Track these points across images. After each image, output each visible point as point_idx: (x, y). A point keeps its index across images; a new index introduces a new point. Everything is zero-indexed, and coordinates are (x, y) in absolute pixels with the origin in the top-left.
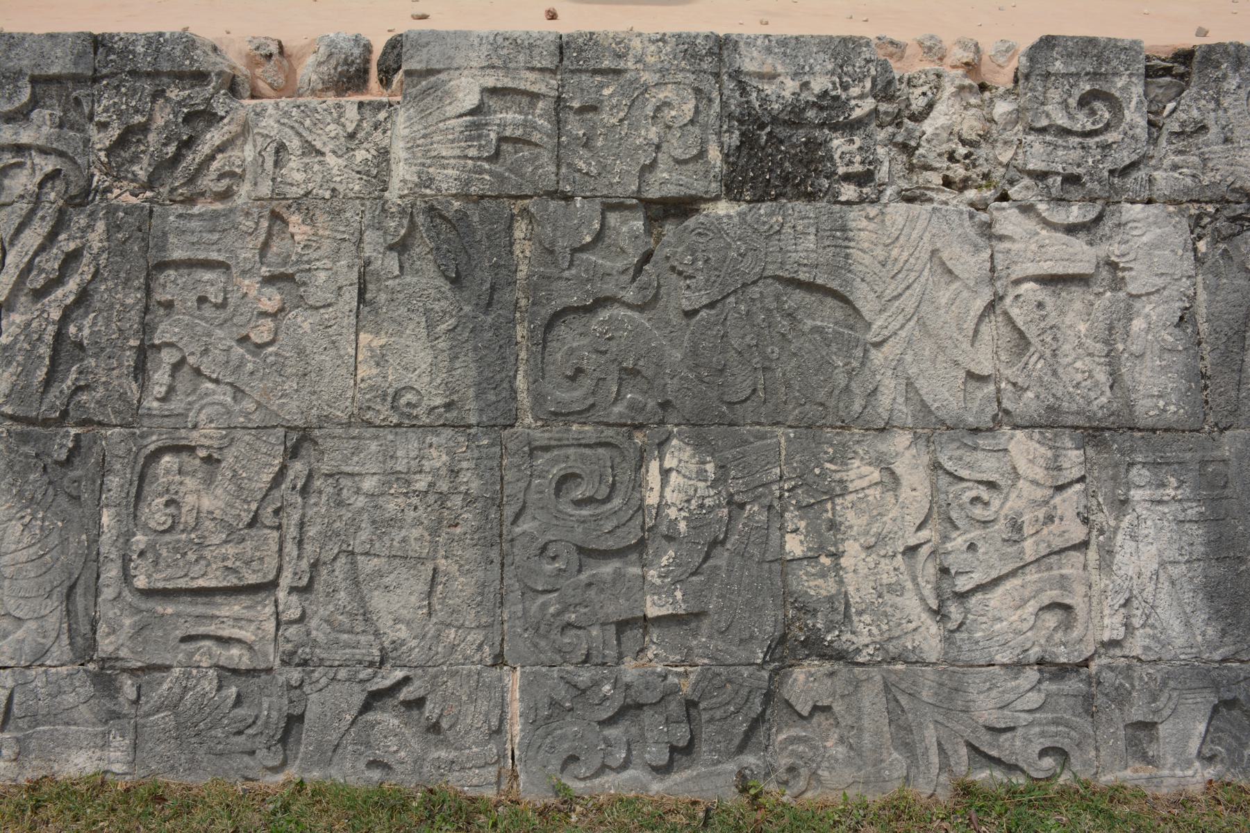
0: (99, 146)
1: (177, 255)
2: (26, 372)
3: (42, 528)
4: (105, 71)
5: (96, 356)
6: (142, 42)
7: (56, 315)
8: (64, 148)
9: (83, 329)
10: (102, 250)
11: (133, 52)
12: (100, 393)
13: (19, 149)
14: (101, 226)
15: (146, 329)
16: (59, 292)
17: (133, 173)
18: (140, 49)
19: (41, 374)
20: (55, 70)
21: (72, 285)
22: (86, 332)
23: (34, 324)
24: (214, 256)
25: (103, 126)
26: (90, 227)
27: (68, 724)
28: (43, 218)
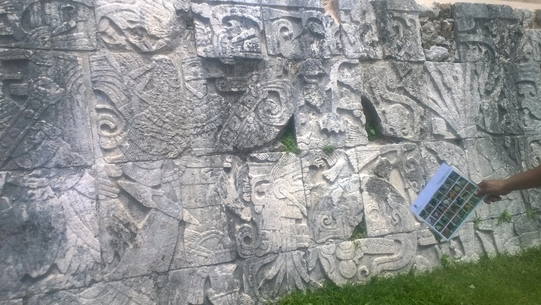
0: (496, 43)
1: (522, 79)
2: (494, 119)
3: (510, 169)
4: (492, 17)
5: (509, 112)
6: (500, 8)
7: (497, 99)
8: (488, 43)
9: (505, 103)
10: (504, 77)
11: (498, 11)
12: (512, 125)
13: (474, 43)
14: (502, 69)
15: (520, 104)
16: (495, 91)
17: (505, 52)
18: (500, 10)
19: (497, 118)
20: (480, 16)
21: (499, 89)
22: (506, 105)
23: (492, 103)
24: (531, 79)
25: (495, 36)
26: (500, 70)
27: (529, 232)
28: (487, 67)
